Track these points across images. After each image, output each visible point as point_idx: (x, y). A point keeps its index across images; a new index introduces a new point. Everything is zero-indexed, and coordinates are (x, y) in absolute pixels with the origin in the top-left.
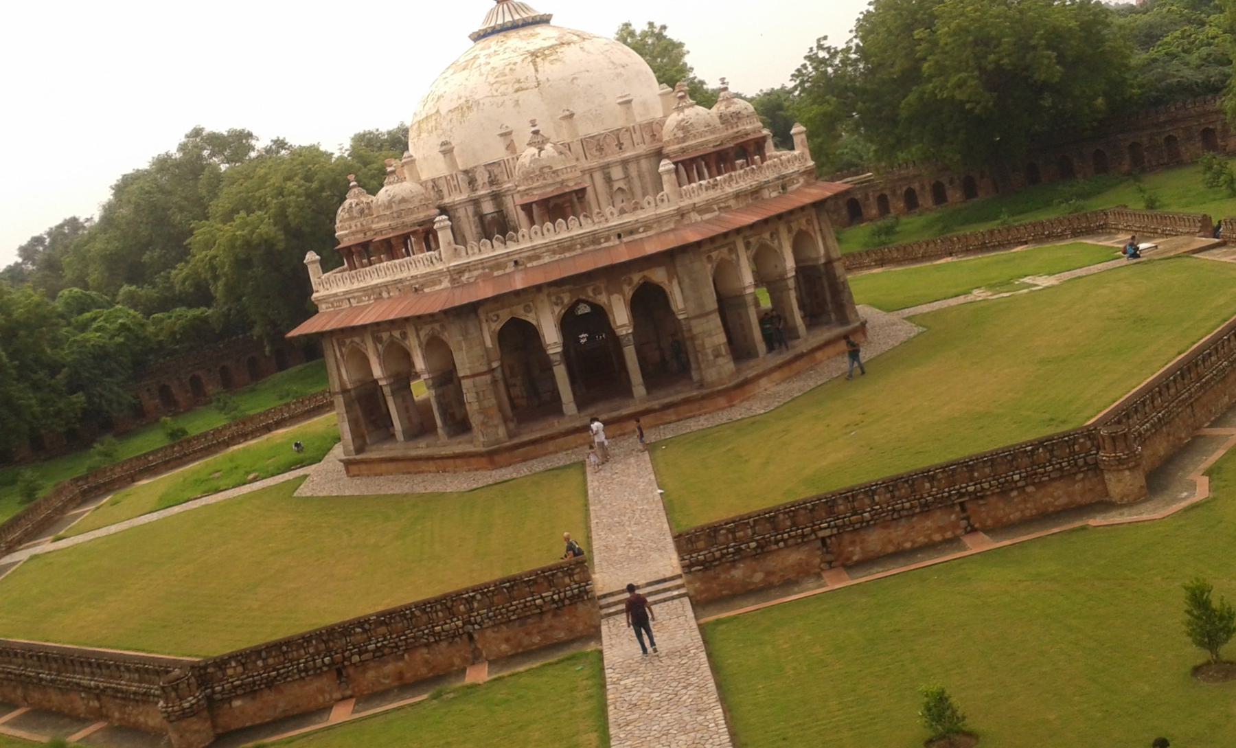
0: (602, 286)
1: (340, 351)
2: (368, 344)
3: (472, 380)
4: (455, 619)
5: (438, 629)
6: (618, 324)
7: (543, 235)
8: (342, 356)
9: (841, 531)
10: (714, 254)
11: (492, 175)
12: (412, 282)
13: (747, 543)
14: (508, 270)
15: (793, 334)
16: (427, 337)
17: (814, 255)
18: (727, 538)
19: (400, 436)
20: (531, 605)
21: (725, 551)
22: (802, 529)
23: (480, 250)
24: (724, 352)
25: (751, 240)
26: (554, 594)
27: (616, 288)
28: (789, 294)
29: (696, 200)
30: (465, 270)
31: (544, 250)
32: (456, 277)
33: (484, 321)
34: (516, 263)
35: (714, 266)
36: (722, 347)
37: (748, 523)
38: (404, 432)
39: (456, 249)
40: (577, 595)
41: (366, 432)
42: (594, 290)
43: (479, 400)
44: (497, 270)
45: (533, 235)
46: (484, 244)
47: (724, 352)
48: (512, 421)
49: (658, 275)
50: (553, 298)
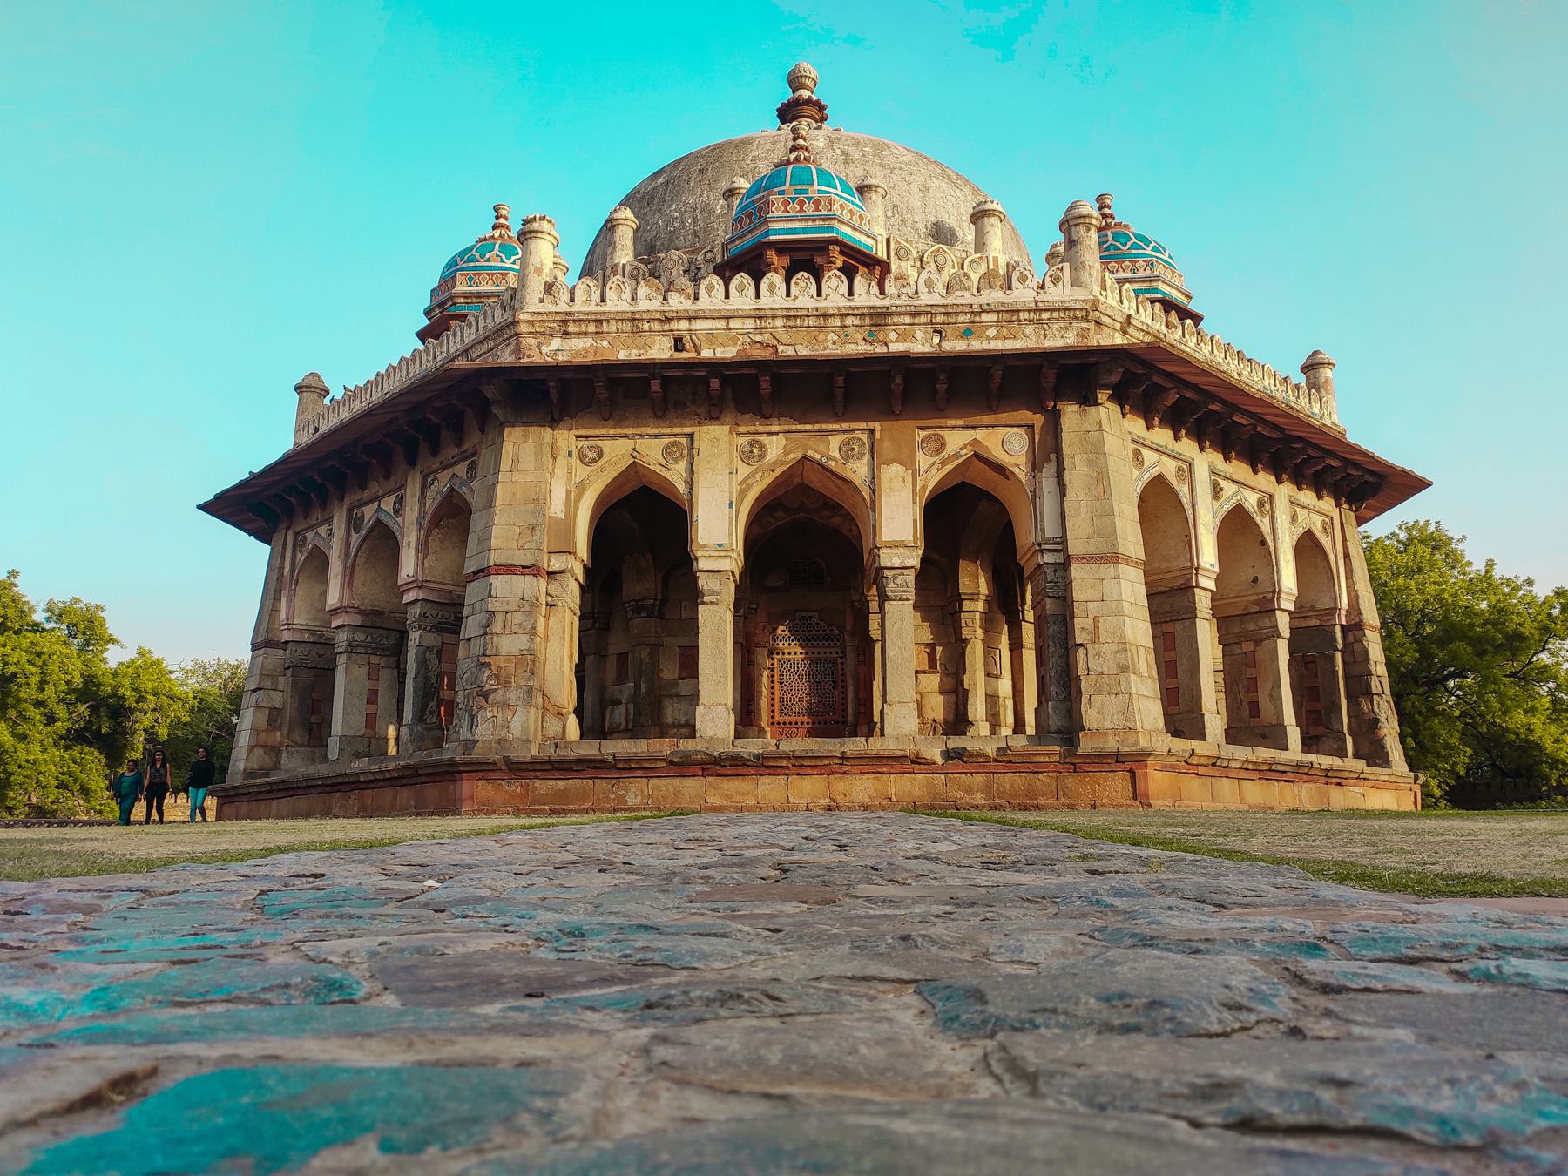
3: (493, 579)
7: (758, 296)
10: (1149, 456)
17: (1326, 603)
23: (603, 300)
24: (1144, 669)
25: (1223, 483)
28: (1275, 650)
29: (1132, 312)
34: (679, 344)
35: (1145, 477)
36: (1142, 651)
41: (287, 742)
45: (732, 287)
47: (1144, 669)
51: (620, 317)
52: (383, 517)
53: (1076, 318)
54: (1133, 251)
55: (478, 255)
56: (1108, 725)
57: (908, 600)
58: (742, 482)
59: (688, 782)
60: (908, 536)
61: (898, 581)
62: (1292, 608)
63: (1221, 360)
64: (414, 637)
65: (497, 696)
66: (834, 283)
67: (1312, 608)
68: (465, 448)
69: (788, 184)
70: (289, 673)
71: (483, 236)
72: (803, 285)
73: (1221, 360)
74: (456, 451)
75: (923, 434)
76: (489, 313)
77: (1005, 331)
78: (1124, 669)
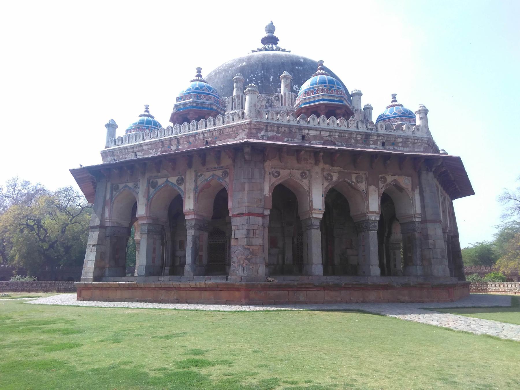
0: (364, 176)
2: (141, 186)
3: (246, 217)
6: (370, 210)
8: (111, 198)
11: (270, 101)
12: (206, 135)
27: (372, 181)
30: (263, 128)
31: (327, 134)
32: (254, 132)
33: (268, 173)
34: (303, 137)
42: (357, 178)
44: (287, 137)
49: (405, 182)
50: (325, 174)
51: (285, 126)
52: (170, 184)
53: (424, 143)
54: (410, 115)
55: (200, 88)
57: (376, 231)
58: (326, 188)
59: (319, 292)
60: (378, 211)
61: (373, 224)
64: (191, 233)
68: (222, 165)
69: (327, 83)
70: (108, 239)
72: (343, 122)
74: (216, 166)
75: (380, 176)
77: (404, 144)
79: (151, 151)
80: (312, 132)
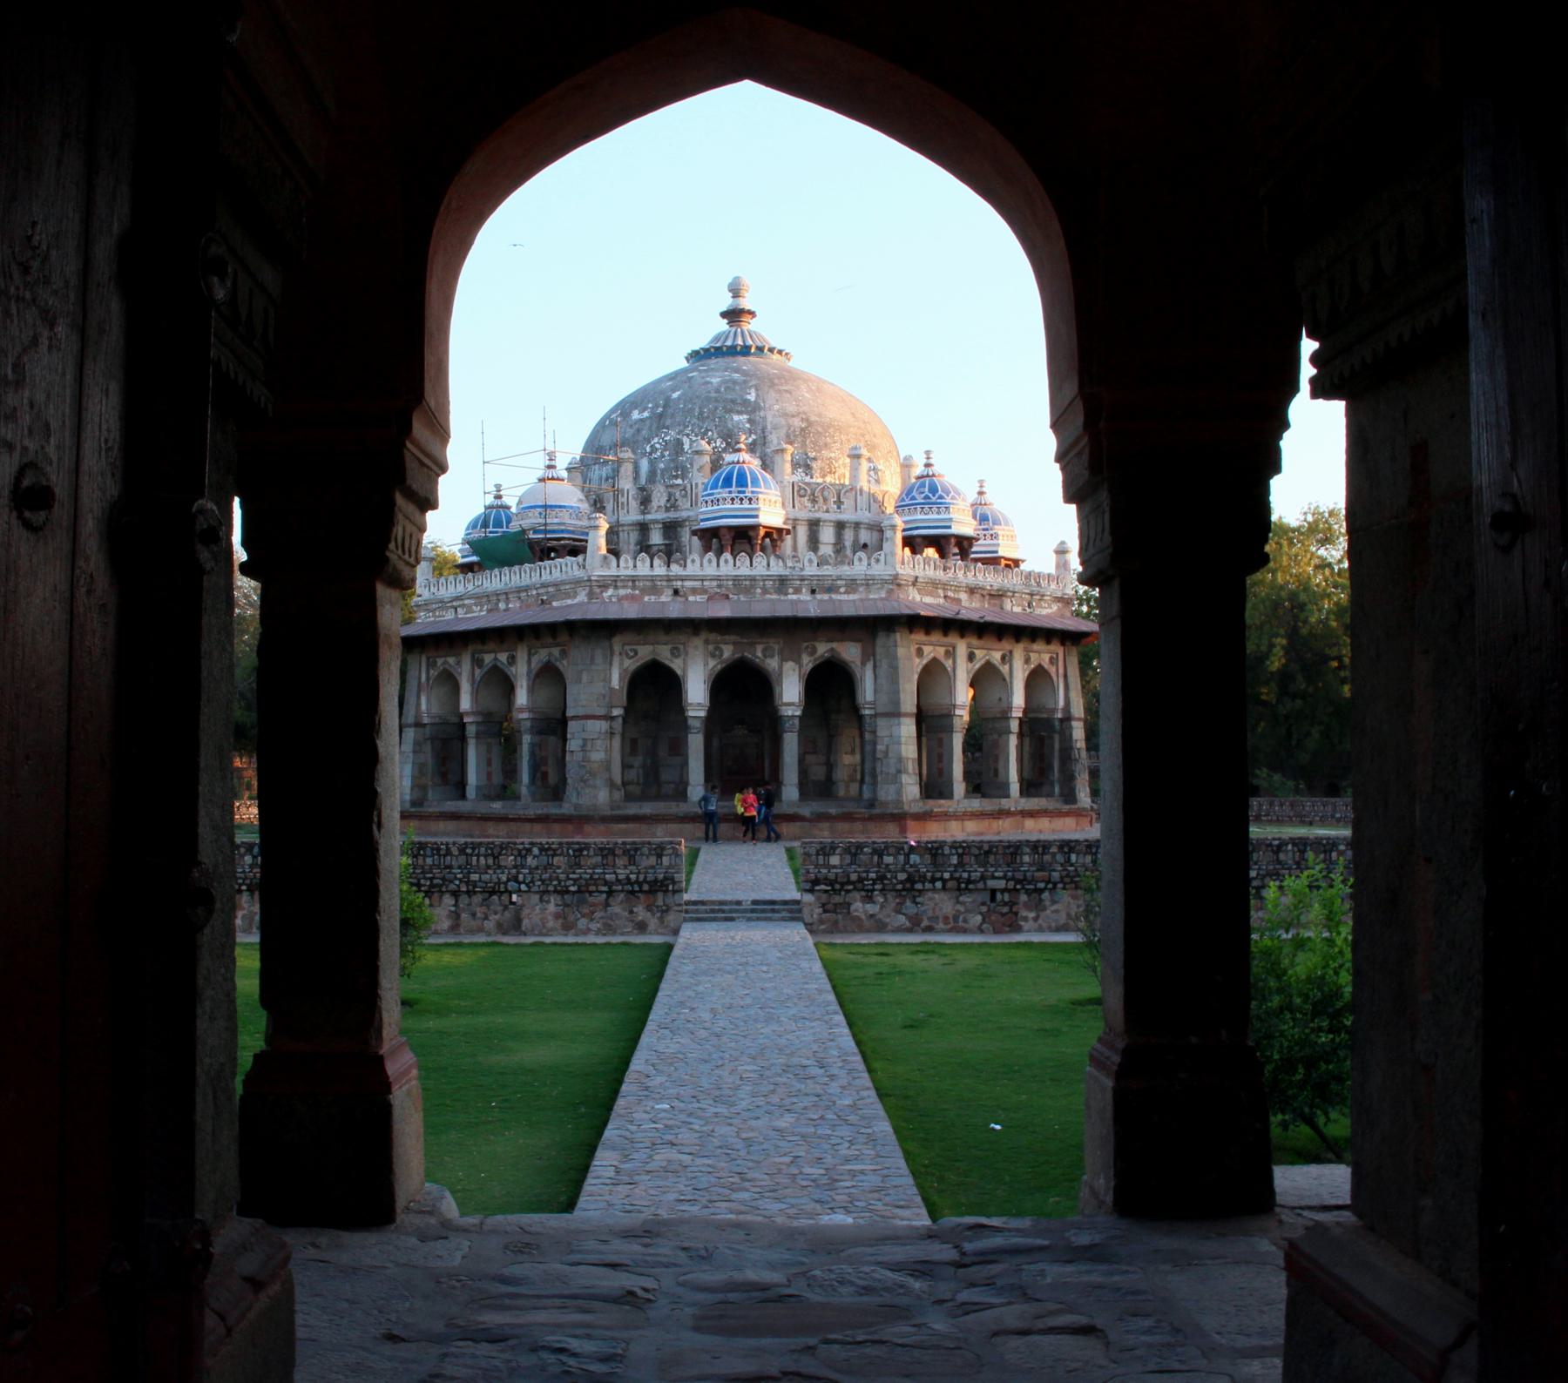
0: (776, 647)
1: (428, 673)
3: (582, 722)
4: (498, 871)
5: (475, 877)
6: (786, 699)
7: (718, 565)
8: (428, 679)
9: (1018, 887)
13: (896, 872)
14: (663, 598)
15: (1003, 791)
16: (540, 665)
17: (1051, 706)
18: (872, 858)
19: (471, 792)
20: (599, 878)
21: (864, 875)
22: (970, 872)
23: (635, 566)
25: (976, 652)
26: (632, 873)
28: (1008, 740)
33: (617, 653)
34: (676, 592)
35: (925, 662)
37: (903, 848)
38: (478, 788)
39: (605, 558)
40: (662, 881)
41: (430, 783)
42: (764, 651)
43: (583, 748)
45: (705, 561)
46: (643, 561)
48: (619, 789)
49: (850, 652)
52: (499, 664)
56: (890, 798)
59: (687, 826)
60: (797, 701)
62: (1020, 715)
63: (980, 578)
64: (527, 739)
65: (591, 782)
66: (760, 559)
67: (1044, 707)
70: (429, 742)
71: (540, 474)
73: (980, 578)
75: (806, 644)
76: (569, 564)
78: (899, 772)
79: (474, 608)
80: (688, 584)
